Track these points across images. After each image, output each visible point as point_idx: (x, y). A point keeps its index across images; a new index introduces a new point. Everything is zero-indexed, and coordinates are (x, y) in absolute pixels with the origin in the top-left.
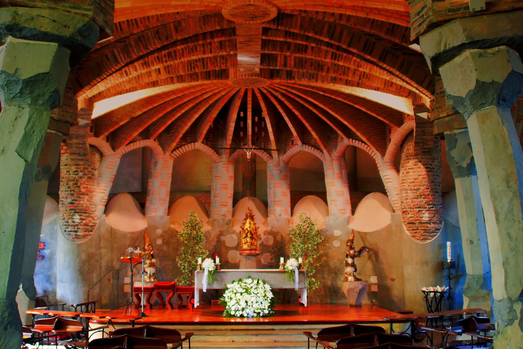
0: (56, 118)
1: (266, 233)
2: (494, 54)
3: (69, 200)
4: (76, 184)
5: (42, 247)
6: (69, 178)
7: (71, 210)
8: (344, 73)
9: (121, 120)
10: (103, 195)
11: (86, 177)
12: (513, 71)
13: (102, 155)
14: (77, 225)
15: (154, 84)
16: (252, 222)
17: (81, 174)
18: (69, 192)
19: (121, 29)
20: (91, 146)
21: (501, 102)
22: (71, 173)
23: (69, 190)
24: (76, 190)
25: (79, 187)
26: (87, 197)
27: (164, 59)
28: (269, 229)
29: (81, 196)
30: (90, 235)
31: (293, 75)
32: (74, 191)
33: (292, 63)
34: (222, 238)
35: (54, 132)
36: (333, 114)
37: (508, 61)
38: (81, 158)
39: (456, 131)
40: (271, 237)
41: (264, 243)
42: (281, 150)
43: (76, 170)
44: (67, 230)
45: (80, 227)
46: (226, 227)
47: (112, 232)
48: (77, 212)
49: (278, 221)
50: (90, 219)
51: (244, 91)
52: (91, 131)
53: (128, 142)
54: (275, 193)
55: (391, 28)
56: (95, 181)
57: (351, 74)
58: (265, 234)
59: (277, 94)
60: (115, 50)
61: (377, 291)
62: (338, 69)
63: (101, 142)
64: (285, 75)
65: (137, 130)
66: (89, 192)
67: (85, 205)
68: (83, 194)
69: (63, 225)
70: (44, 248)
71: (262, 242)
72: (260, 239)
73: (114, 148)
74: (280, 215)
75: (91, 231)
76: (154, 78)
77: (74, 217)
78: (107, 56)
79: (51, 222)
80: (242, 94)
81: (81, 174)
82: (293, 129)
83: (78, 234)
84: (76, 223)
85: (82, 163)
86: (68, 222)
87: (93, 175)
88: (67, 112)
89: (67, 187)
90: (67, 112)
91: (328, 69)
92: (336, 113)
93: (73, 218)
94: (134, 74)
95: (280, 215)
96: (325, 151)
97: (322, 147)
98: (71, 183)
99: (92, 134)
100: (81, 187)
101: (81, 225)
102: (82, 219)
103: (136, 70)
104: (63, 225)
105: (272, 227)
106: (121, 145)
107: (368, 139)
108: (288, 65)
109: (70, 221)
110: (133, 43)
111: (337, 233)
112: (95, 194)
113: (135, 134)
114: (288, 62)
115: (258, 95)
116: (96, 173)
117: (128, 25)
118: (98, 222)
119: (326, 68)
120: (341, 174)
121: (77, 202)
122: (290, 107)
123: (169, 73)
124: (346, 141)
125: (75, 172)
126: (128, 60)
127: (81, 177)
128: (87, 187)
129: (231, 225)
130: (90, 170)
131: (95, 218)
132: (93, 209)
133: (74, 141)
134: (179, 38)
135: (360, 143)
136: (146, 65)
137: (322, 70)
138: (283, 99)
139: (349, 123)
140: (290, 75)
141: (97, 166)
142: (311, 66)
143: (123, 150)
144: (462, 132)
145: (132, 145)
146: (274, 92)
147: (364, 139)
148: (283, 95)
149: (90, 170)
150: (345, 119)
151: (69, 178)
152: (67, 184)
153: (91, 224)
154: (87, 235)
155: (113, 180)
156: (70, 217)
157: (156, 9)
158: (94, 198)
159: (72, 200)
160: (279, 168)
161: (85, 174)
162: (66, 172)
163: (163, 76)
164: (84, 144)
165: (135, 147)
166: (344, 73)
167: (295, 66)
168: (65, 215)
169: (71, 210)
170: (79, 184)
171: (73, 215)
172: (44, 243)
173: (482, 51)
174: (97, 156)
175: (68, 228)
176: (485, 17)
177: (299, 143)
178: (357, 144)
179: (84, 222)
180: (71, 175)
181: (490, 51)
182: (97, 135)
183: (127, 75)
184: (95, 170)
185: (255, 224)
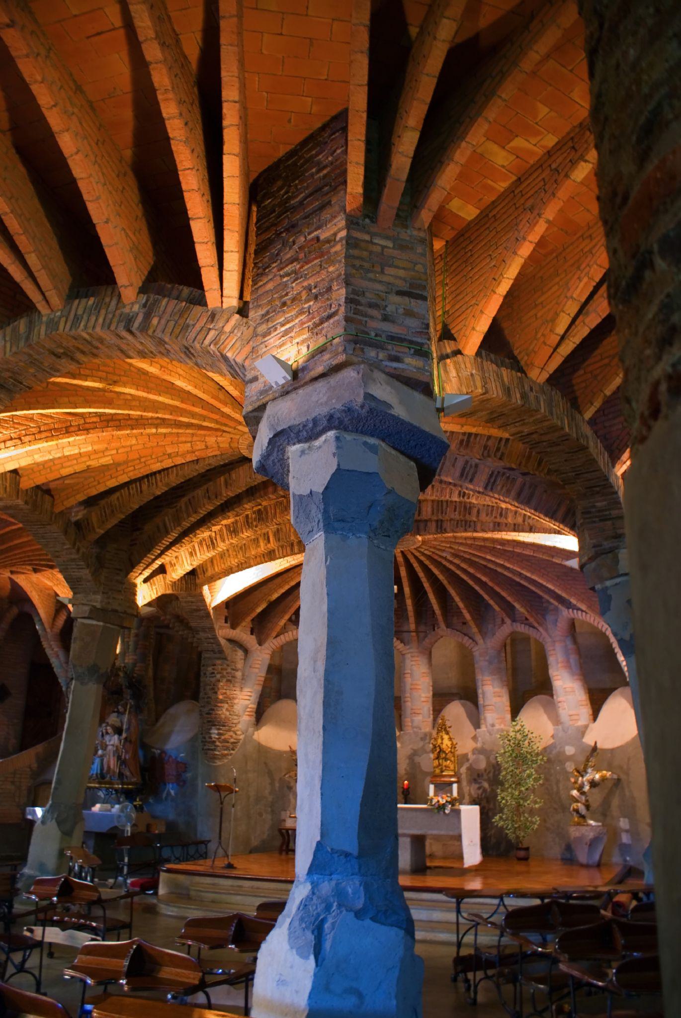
0: (98, 606)
1: (475, 751)
2: (320, 447)
8: (501, 515)
9: (257, 605)
10: (247, 702)
11: (225, 680)
12: (338, 470)
13: (246, 651)
14: (214, 742)
15: (270, 556)
16: (446, 737)
17: (218, 676)
19: (141, 492)
20: (230, 641)
21: (336, 524)
22: (208, 673)
25: (216, 693)
26: (226, 706)
27: (254, 523)
28: (479, 745)
30: (231, 754)
31: (445, 525)
33: (429, 509)
34: (417, 759)
35: (101, 624)
36: (529, 575)
37: (334, 454)
38: (217, 655)
39: (608, 583)
40: (482, 757)
41: (475, 766)
42: (483, 634)
45: (218, 743)
46: (421, 744)
47: (262, 751)
48: (215, 725)
49: (491, 734)
50: (231, 733)
51: (400, 554)
52: (226, 622)
53: (274, 634)
54: (483, 693)
55: (465, 438)
56: (237, 685)
57: (510, 515)
58: (474, 754)
59: (444, 555)
60: (166, 519)
61: (630, 842)
62: (492, 511)
63: (242, 633)
64: (433, 526)
65: (282, 618)
66: (229, 700)
67: (223, 716)
68: (222, 702)
71: (471, 765)
72: (468, 760)
73: (260, 644)
74: (493, 725)
75: (233, 750)
76: (263, 547)
78: (158, 527)
80: (400, 559)
82: (491, 602)
85: (219, 662)
87: (234, 677)
88: (114, 598)
90: (114, 598)
91: (478, 512)
92: (533, 573)
94: (222, 546)
95: (493, 725)
96: (541, 629)
97: (536, 625)
99: (228, 625)
102: (219, 734)
103: (224, 541)
105: (483, 743)
106: (268, 636)
107: (589, 607)
108: (424, 513)
109: (207, 737)
110: (183, 507)
111: (570, 750)
112: (236, 701)
113: (282, 622)
114: (424, 509)
115: (422, 558)
116: (239, 674)
117: (149, 486)
118: (242, 737)
119: (475, 511)
120: (568, 661)
122: (471, 570)
123: (279, 540)
124: (566, 613)
125: (213, 673)
126: (179, 529)
128: (225, 693)
129: (427, 741)
130: (229, 670)
131: (238, 733)
132: (235, 721)
133: (202, 635)
134: (231, 494)
135: (580, 612)
136: (233, 531)
137: (470, 514)
138: (457, 561)
139: (554, 585)
140: (440, 527)
141: (240, 665)
142: (455, 511)
143: (272, 644)
144: (616, 584)
145: (282, 636)
146: (437, 552)
147: (583, 607)
148: (455, 555)
149: (229, 670)
150: (548, 581)
153: (232, 740)
154: (227, 755)
155: (262, 683)
157: (161, 462)
158: (235, 707)
160: (487, 658)
161: (223, 677)
163: (273, 545)
164: (215, 638)
165: (288, 639)
166: (501, 515)
167: (433, 514)
171: (210, 729)
173: (306, 445)
174: (240, 653)
176: (300, 391)
177: (508, 621)
178: (579, 615)
179: (223, 737)
181: (317, 443)
182: (233, 627)
183: (214, 548)
184: (237, 670)
185: (450, 739)
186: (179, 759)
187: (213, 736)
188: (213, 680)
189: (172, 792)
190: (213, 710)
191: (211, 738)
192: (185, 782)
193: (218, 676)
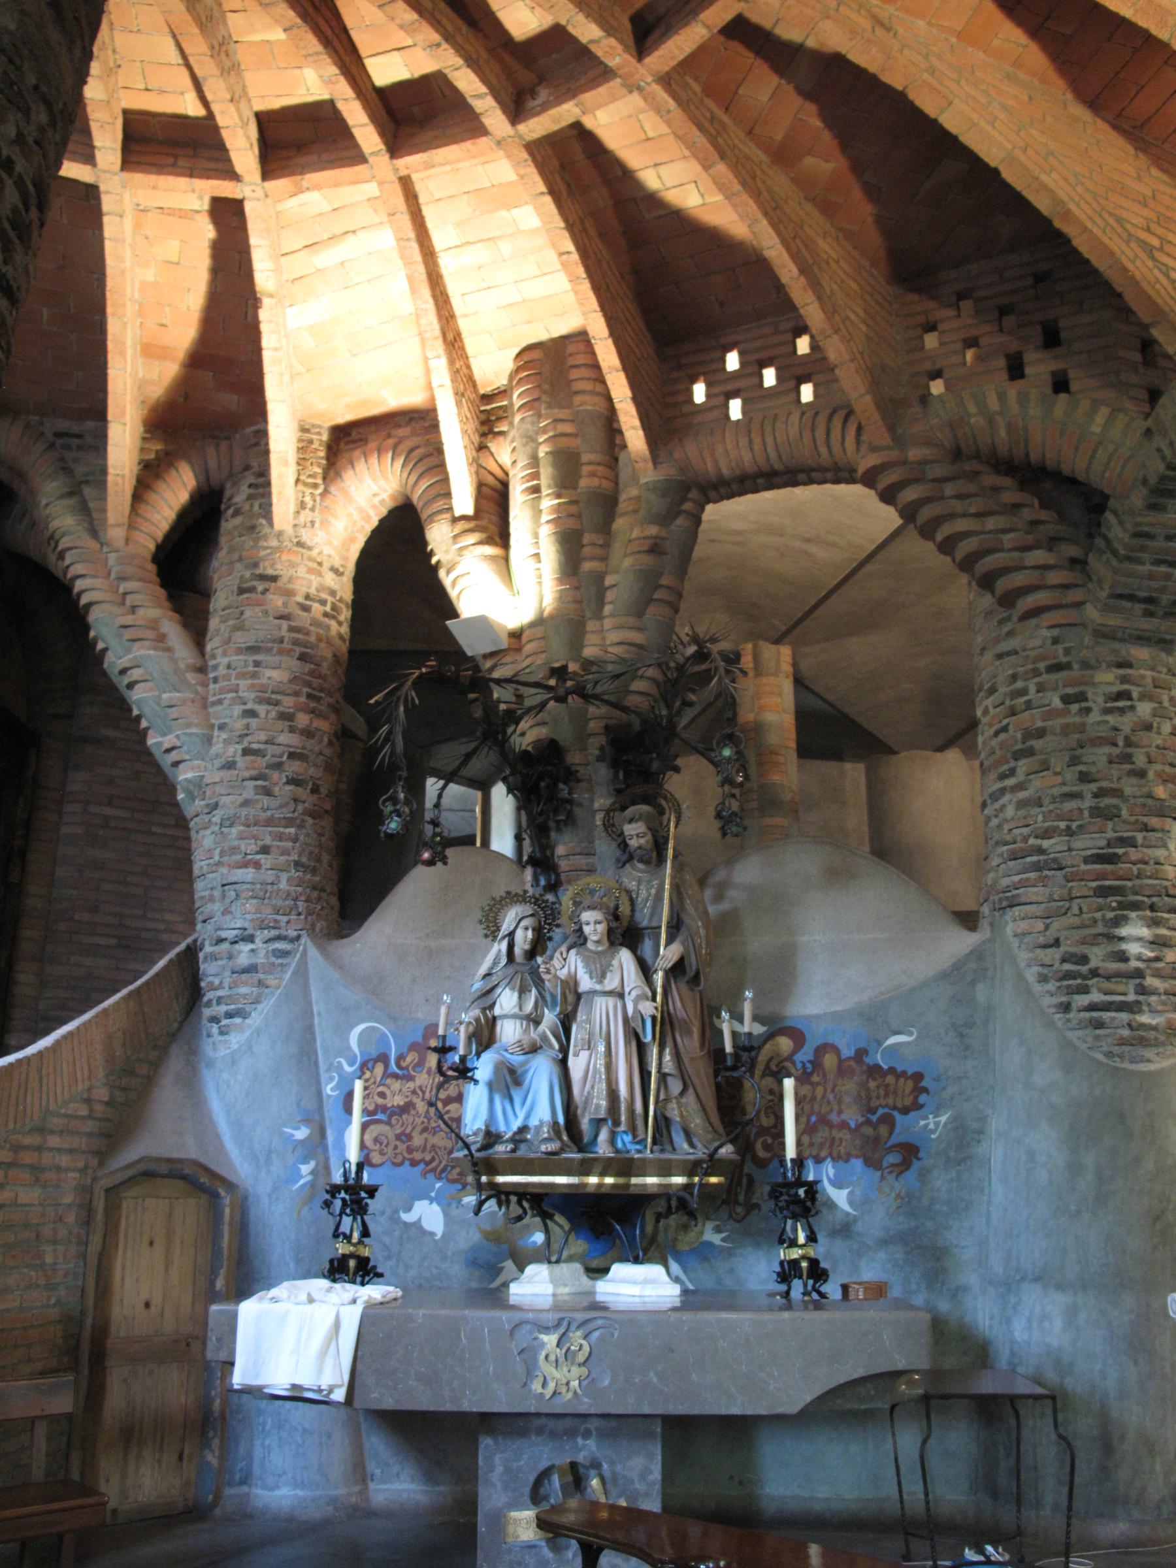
3: (1090, 842)
4: (1127, 758)
5: (908, 1101)
6: (1082, 728)
7: (1103, 892)
14: (1139, 974)
18: (1088, 802)
22: (1096, 700)
23: (1089, 788)
24: (1130, 787)
25: (1141, 774)
29: (1154, 822)
32: (1117, 793)
43: (1115, 689)
44: (1082, 1000)
45: (1151, 981)
48: (1135, 906)
69: (1043, 979)
70: (917, 1106)
77: (1124, 931)
79: (958, 966)
81: (1144, 709)
83: (1145, 1019)
84: (1134, 964)
85: (1141, 653)
86: (1084, 960)
89: (1070, 774)
93: (1111, 938)
98: (1099, 756)
100: (1151, 775)
101: (1158, 974)
102: (1158, 943)
104: (1043, 979)
109: (1097, 956)
121: (1134, 855)
125: (1120, 696)
127: (1148, 728)
151: (1082, 728)
152: (1074, 761)
156: (1100, 929)
159: (1109, 845)
162: (1057, 703)
168: (1057, 924)
169: (1103, 892)
170: (1140, 760)
171: (1118, 922)
172: (918, 1077)
175: (1084, 990)
180: (1095, 717)
186: (879, 1059)
187: (1133, 948)
188: (1125, 723)
189: (840, 1197)
190: (1131, 843)
191: (1123, 957)
192: (909, 1152)
193: (1144, 709)
